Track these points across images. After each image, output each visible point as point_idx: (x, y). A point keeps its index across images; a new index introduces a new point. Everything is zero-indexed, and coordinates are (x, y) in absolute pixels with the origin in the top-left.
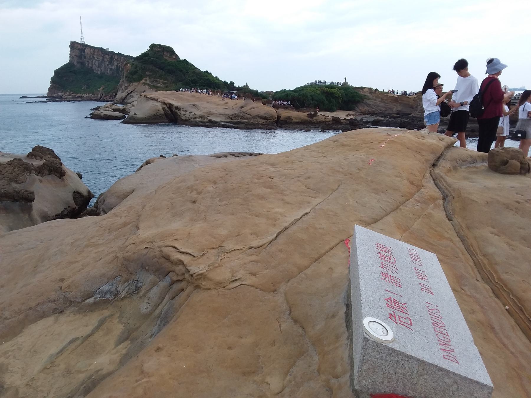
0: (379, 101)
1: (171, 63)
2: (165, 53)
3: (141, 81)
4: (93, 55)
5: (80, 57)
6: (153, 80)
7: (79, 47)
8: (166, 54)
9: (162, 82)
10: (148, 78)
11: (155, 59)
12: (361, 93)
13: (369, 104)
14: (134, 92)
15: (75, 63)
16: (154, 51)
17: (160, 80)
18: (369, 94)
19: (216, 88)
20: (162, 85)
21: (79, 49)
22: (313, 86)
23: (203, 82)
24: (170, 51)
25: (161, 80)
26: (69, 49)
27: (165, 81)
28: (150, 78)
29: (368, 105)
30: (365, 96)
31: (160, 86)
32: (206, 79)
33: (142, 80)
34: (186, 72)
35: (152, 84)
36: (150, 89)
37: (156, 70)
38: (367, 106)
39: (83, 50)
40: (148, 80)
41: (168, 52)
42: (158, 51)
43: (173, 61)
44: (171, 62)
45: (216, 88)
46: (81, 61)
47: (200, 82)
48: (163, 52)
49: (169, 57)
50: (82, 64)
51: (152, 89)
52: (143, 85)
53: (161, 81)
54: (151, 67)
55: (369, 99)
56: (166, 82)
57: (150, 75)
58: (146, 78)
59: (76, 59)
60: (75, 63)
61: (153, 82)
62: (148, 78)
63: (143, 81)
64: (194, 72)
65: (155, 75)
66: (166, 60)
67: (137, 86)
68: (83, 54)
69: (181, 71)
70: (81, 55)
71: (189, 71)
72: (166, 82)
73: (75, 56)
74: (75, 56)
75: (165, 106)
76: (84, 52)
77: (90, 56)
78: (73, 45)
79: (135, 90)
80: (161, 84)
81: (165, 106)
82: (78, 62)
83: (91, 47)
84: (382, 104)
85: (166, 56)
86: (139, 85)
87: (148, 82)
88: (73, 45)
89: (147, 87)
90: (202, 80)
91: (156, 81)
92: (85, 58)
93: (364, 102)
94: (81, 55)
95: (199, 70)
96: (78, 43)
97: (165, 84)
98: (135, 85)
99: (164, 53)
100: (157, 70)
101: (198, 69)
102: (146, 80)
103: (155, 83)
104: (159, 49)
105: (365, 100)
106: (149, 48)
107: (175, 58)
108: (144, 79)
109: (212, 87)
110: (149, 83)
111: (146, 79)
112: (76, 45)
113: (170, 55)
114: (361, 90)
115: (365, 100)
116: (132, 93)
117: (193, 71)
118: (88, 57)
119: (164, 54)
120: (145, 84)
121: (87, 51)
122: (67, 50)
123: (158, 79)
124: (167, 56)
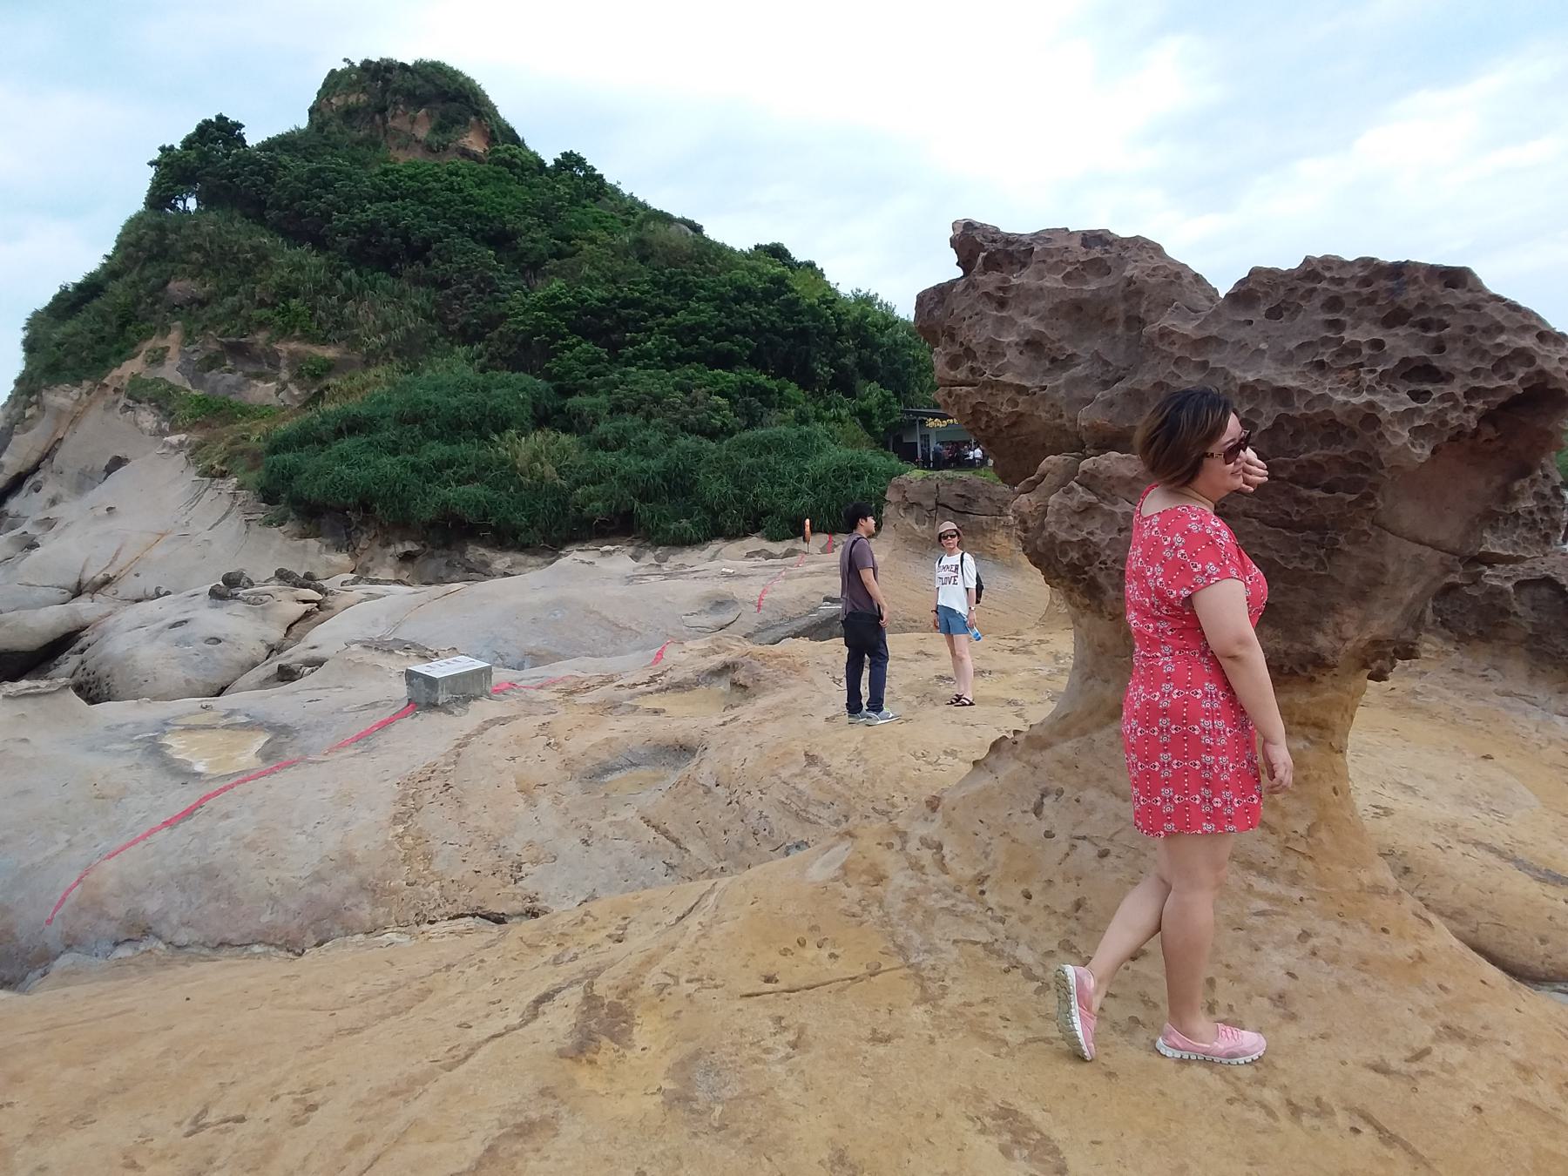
1: (411, 178)
3: (116, 372)
6: (214, 346)
8: (407, 127)
9: (291, 353)
14: (39, 476)
17: (270, 340)
19: (860, 383)
20: (291, 386)
23: (707, 312)
25: (284, 333)
27: (324, 342)
28: (188, 335)
31: (274, 401)
33: (122, 355)
35: (197, 380)
36: (161, 433)
37: (255, 241)
40: (173, 352)
41: (415, 99)
44: (411, 171)
45: (860, 383)
47: (681, 316)
48: (382, 111)
49: (429, 149)
51: (174, 439)
52: (123, 400)
53: (284, 348)
56: (330, 353)
57: (202, 303)
58: (164, 336)
61: (212, 362)
63: (132, 367)
64: (643, 251)
65: (230, 301)
67: (75, 420)
69: (501, 240)
71: (592, 240)
72: (330, 353)
79: (48, 455)
80: (285, 375)
85: (410, 141)
86: (90, 404)
87: (170, 372)
89: (148, 419)
90: (693, 304)
91: (238, 351)
95: (697, 229)
97: (317, 377)
98: (60, 412)
99: (385, 122)
100: (254, 249)
101: (683, 221)
102: (158, 359)
103: (224, 380)
104: (352, 99)
109: (823, 371)
111: (162, 344)
113: (434, 131)
116: (29, 483)
119: (391, 123)
120: (138, 393)
123: (261, 337)
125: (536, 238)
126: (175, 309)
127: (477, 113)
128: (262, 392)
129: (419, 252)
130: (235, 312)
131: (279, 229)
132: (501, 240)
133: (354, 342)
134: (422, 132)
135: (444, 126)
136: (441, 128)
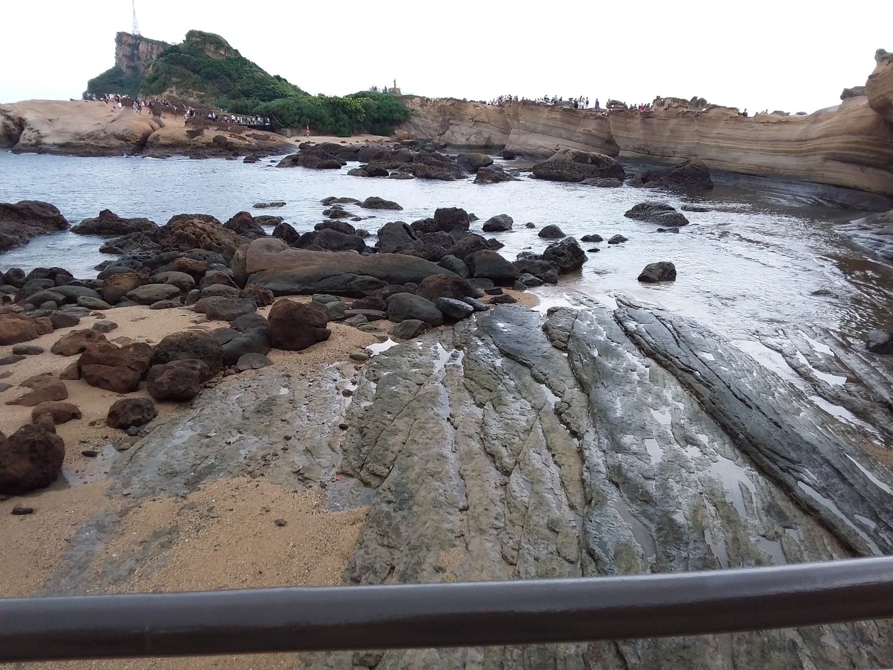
0: (431, 120)
2: (208, 46)
4: (151, 53)
5: (131, 57)
7: (130, 41)
10: (174, 88)
11: (187, 55)
12: (409, 106)
13: (418, 125)
15: (124, 69)
16: (190, 43)
18: (419, 108)
21: (130, 45)
22: (371, 95)
24: (217, 42)
25: (195, 90)
26: (114, 45)
28: (177, 88)
29: (416, 127)
30: (413, 110)
32: (268, 89)
33: (164, 91)
34: (239, 78)
38: (415, 129)
39: (135, 47)
41: (211, 43)
42: (197, 42)
43: (221, 58)
46: (133, 65)
49: (214, 52)
50: (135, 69)
53: (195, 92)
54: (179, 68)
55: (419, 116)
59: (125, 62)
60: (122, 68)
61: (182, 94)
62: (174, 88)
63: (166, 93)
66: (208, 56)
68: (136, 52)
69: (229, 75)
70: (133, 54)
73: (124, 56)
74: (124, 56)
75: (8, 122)
76: (138, 49)
77: (146, 56)
78: (121, 38)
81: (8, 122)
82: (128, 67)
83: (148, 41)
84: (436, 124)
85: (210, 51)
87: (174, 94)
88: (121, 38)
91: (187, 92)
92: (139, 58)
93: (412, 121)
94: (133, 54)
96: (129, 35)
102: (171, 92)
103: (185, 97)
105: (412, 117)
106: (185, 38)
107: (223, 53)
108: (168, 89)
110: (175, 96)
112: (125, 38)
114: (409, 101)
115: (412, 117)
117: (250, 75)
118: (143, 57)
121: (142, 47)
122: (111, 47)
124: (210, 51)
125: (235, 75)
126: (174, 83)
127: (223, 46)
128: (191, 99)
129: (216, 78)
130: (185, 85)
131: (192, 71)
132: (229, 75)
133: (207, 92)
134: (212, 49)
135: (217, 48)
136: (216, 49)
